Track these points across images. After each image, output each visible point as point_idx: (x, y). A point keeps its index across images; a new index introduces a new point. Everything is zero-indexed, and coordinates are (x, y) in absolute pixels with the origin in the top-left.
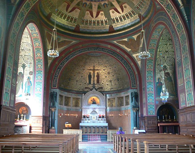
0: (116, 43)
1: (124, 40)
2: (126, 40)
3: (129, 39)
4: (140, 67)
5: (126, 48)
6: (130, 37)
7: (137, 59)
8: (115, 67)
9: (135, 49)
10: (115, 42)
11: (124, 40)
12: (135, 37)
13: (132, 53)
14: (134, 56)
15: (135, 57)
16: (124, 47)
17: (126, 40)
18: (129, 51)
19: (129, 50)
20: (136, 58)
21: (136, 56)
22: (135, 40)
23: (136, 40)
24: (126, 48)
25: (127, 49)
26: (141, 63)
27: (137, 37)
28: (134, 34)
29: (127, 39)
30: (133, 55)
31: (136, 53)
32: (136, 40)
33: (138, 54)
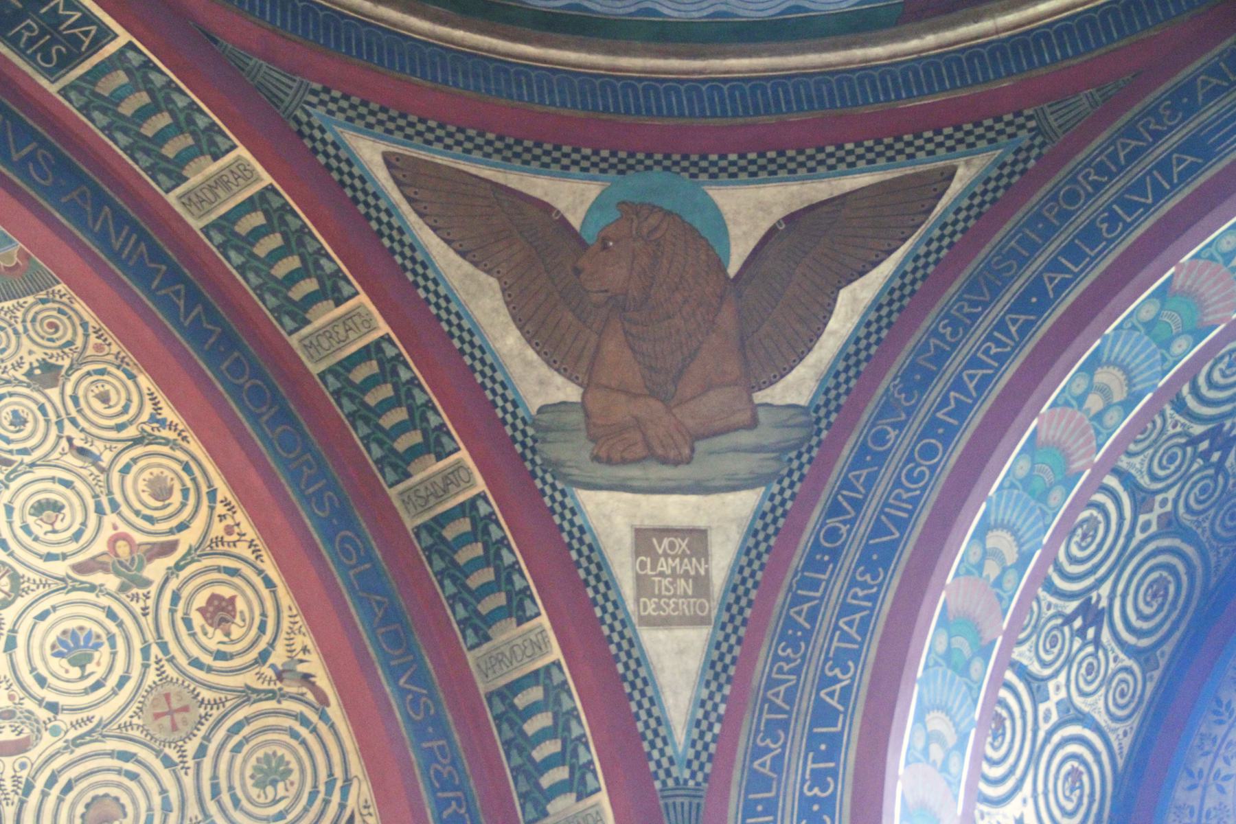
0: (382, 176)
1: (540, 186)
2: (573, 197)
3: (629, 209)
4: (680, 736)
5: (508, 342)
6: (657, 175)
7: (642, 584)
8: (75, 648)
9: (650, 408)
10: (369, 152)
11: (540, 186)
12: (748, 211)
13: (572, 451)
14: (612, 515)
15: (628, 539)
16: (483, 301)
17: (573, 197)
18: (534, 403)
19: (540, 385)
20: (624, 569)
21: (644, 539)
22: (721, 267)
23: (732, 270)
24: (508, 342)
25: (515, 369)
26: (716, 668)
27: (790, 219)
28: (763, 159)
29: (591, 190)
30: (583, 495)
31: (658, 472)
32: (732, 270)
33: (676, 509)
